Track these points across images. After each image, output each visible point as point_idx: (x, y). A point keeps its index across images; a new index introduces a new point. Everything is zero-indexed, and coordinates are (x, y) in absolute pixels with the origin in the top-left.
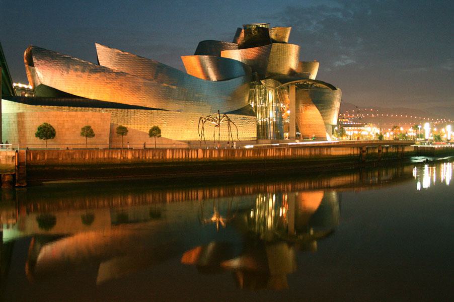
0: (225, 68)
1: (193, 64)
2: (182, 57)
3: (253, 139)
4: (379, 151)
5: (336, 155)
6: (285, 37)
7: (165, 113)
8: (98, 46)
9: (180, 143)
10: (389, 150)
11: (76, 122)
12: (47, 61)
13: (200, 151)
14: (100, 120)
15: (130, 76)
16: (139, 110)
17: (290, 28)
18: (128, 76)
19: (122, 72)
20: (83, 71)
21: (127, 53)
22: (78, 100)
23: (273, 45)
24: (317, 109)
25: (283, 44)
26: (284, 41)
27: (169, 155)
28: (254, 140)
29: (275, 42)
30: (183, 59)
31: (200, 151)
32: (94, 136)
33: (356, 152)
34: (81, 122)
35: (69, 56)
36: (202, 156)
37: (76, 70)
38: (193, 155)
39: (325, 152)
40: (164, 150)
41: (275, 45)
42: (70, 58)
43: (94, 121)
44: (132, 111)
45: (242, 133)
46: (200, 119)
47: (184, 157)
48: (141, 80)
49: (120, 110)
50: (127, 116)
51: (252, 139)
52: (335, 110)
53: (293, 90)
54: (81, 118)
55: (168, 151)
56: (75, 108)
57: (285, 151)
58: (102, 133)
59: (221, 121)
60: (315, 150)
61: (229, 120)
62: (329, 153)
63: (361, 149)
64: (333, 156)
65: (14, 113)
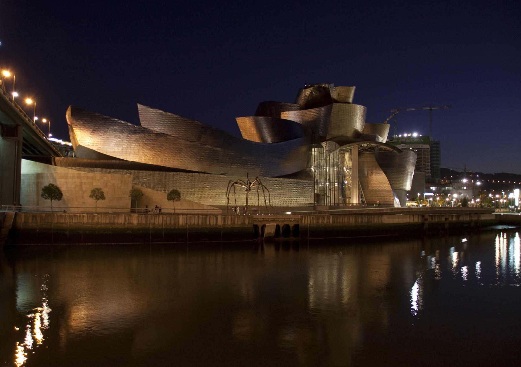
0: (285, 131)
1: (247, 127)
2: (237, 118)
3: (310, 205)
4: (446, 219)
5: (390, 224)
6: (348, 97)
7: (207, 177)
8: (139, 106)
9: (212, 208)
10: (461, 218)
12: (86, 121)
13: (220, 218)
15: (170, 137)
16: (178, 173)
17: (354, 87)
18: (168, 137)
19: (163, 134)
20: (122, 132)
21: (169, 114)
22: (114, 161)
23: (334, 105)
24: (384, 174)
25: (345, 104)
26: (347, 101)
27: (182, 221)
28: (311, 206)
29: (336, 102)
30: (237, 121)
32: (103, 198)
33: (416, 220)
35: (108, 117)
36: (222, 223)
37: (115, 131)
38: (212, 222)
39: (376, 220)
40: (176, 215)
41: (335, 106)
43: (114, 184)
44: (171, 173)
45: (287, 199)
46: (229, 183)
47: (200, 223)
48: (182, 142)
49: (158, 172)
50: (165, 179)
51: (308, 205)
52: (408, 174)
53: (355, 152)
54: (99, 180)
55: (181, 217)
56: (109, 170)
57: (324, 219)
59: (252, 185)
60: (362, 218)
61: (260, 184)
62: (380, 221)
63: (423, 216)
64: (385, 224)
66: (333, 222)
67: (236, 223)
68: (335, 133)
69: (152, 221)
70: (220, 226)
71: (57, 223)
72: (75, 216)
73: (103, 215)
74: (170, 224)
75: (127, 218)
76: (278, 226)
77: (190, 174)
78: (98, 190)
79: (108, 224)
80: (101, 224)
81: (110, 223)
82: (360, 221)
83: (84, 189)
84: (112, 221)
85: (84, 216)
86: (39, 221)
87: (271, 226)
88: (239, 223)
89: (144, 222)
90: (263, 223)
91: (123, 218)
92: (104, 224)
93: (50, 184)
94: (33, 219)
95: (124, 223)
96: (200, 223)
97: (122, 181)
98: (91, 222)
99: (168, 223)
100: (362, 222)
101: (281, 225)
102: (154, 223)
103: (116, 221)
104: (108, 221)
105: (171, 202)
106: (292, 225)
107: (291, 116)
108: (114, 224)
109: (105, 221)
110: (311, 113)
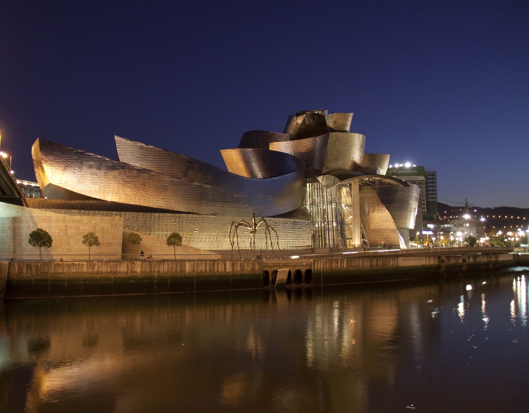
0: (275, 164)
1: (233, 159)
2: (221, 151)
3: (307, 248)
4: (464, 261)
5: (405, 267)
6: (345, 125)
7: (196, 218)
8: (117, 138)
9: (210, 253)
10: (478, 260)
11: (81, 228)
12: (57, 156)
13: (228, 264)
14: (110, 225)
15: (154, 174)
16: (164, 214)
17: (352, 114)
18: (152, 173)
19: (146, 169)
20: (99, 168)
21: (152, 147)
22: (91, 202)
23: (330, 135)
24: (387, 211)
25: (342, 133)
26: (344, 129)
27: (188, 268)
28: (309, 249)
29: (333, 130)
30: (222, 153)
31: (228, 264)
32: (98, 244)
33: (432, 262)
34: (87, 228)
35: (82, 151)
36: (231, 270)
37: (91, 167)
38: (220, 268)
39: (391, 263)
40: (183, 262)
41: (332, 135)
42: (84, 153)
43: (103, 227)
44: (157, 215)
45: (287, 241)
46: (232, 224)
47: (208, 270)
48: (167, 178)
49: (142, 213)
50: (150, 221)
51: (305, 248)
52: (411, 211)
53: (356, 186)
54: (86, 224)
55: (187, 264)
56: (87, 212)
57: (338, 263)
58: (113, 241)
59: (258, 226)
60: (377, 261)
61: (267, 226)
62: (396, 264)
63: (439, 258)
64: (402, 267)
65: (9, 218)
66: (347, 266)
67: (246, 269)
68: (332, 165)
69: (157, 269)
70: (229, 273)
71: (54, 273)
72: (74, 264)
73: (104, 263)
74: (176, 271)
75: (130, 266)
76: (290, 272)
77: (177, 215)
78: (91, 234)
79: (109, 273)
80: (102, 274)
81: (111, 272)
82: (375, 264)
83: (70, 234)
84: (114, 270)
85: (83, 265)
86: (34, 270)
87: (283, 271)
88: (249, 269)
89: (148, 270)
90: (275, 269)
91: (126, 266)
92: (105, 273)
93: (38, 229)
94: (27, 270)
95: (127, 272)
96: (208, 270)
97: (112, 224)
98: (91, 271)
99: (174, 271)
100: (377, 265)
101: (293, 270)
102: (159, 271)
103: (118, 269)
104: (109, 270)
105: (172, 247)
106: (303, 270)
107: (282, 147)
108: (116, 273)
109: (106, 270)
110: (306, 144)
